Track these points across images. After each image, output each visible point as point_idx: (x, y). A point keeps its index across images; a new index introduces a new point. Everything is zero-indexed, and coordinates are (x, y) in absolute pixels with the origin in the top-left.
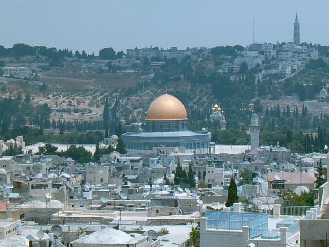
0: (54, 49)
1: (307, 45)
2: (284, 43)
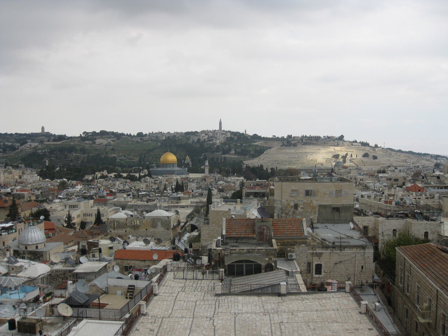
0: (118, 132)
1: (225, 131)
2: (215, 130)
